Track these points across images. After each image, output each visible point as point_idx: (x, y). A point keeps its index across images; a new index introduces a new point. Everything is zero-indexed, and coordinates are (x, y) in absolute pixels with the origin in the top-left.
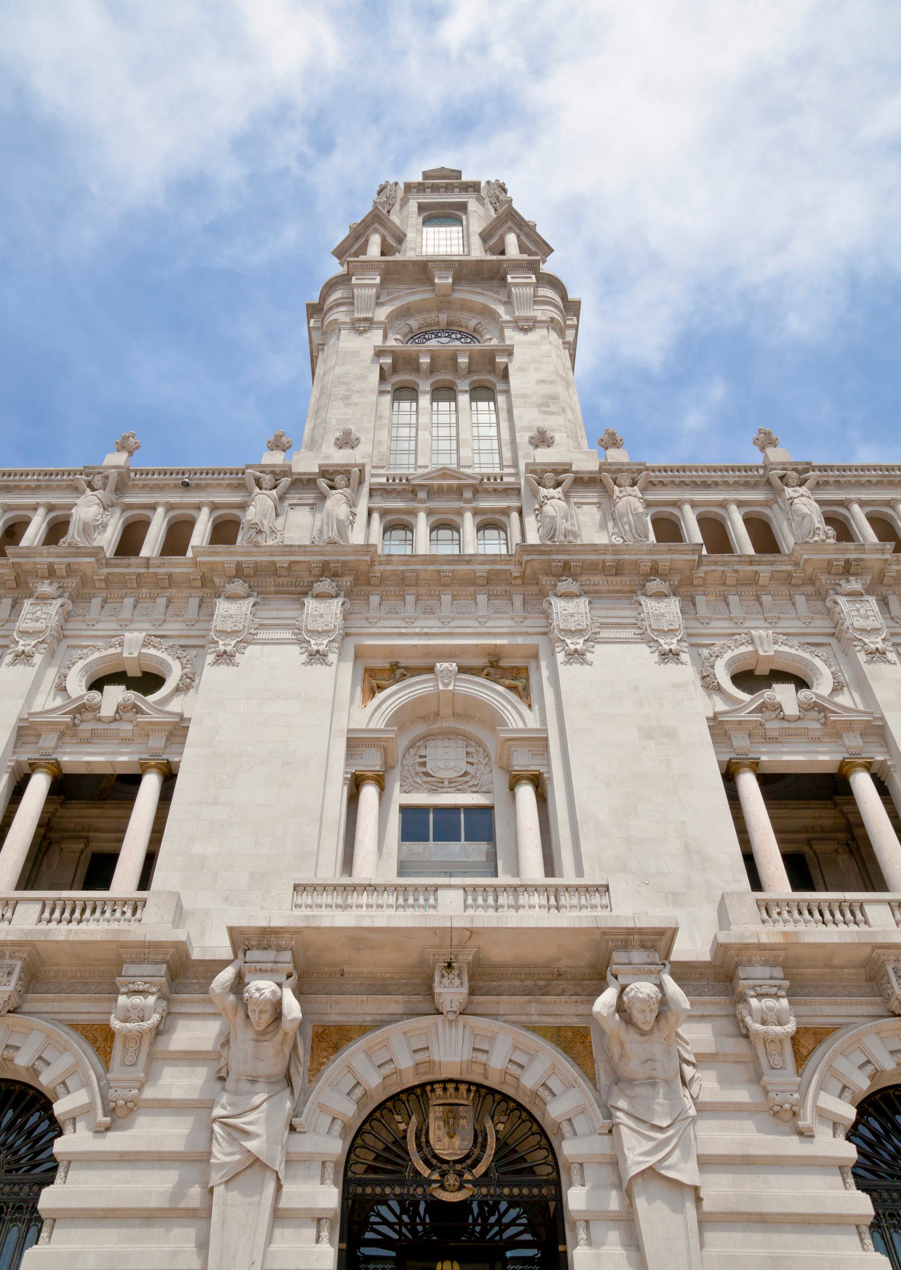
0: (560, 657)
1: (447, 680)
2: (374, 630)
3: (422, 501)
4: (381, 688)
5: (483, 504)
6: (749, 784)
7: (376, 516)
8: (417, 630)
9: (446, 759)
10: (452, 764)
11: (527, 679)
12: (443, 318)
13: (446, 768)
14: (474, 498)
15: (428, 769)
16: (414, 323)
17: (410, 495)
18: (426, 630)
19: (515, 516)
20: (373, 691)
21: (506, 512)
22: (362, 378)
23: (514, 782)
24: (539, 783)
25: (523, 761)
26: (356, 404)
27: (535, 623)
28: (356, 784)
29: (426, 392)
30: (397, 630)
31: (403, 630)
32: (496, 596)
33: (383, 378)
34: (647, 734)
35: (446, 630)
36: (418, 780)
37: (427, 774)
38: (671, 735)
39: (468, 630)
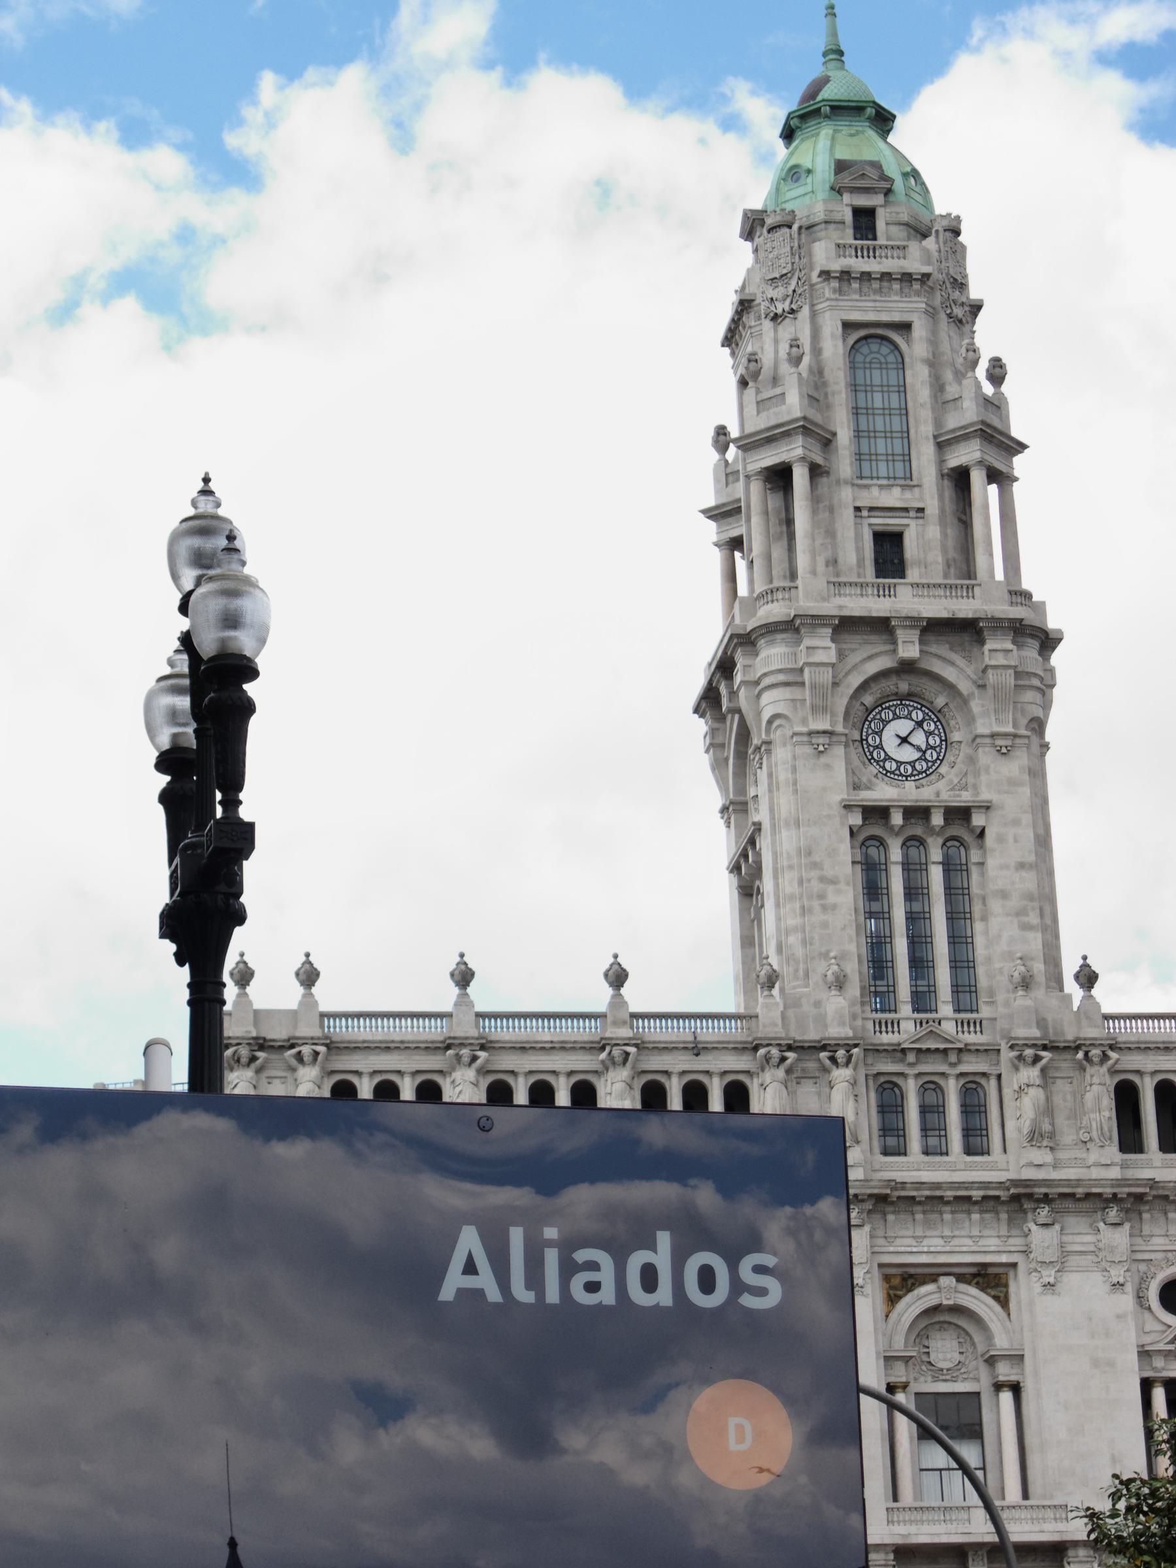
0: (1038, 1288)
1: (945, 1291)
2: (892, 1249)
3: (911, 1065)
4: (900, 1298)
5: (964, 1068)
6: (1159, 1396)
7: (871, 1082)
8: (925, 1249)
9: (944, 1349)
10: (949, 1356)
11: (1006, 1286)
12: (904, 687)
13: (945, 1360)
14: (959, 1062)
15: (931, 1360)
16: (868, 700)
17: (899, 1055)
18: (932, 1249)
19: (993, 1082)
20: (892, 1299)
21: (984, 1074)
22: (832, 853)
23: (998, 1387)
24: (1016, 1389)
25: (1005, 1372)
26: (834, 907)
27: (1016, 1242)
29: (897, 863)
30: (909, 1249)
31: (915, 1250)
32: (987, 1211)
33: (852, 834)
34: (1096, 1363)
35: (948, 1249)
36: (924, 1368)
37: (930, 1363)
38: (1111, 1364)
39: (964, 1249)
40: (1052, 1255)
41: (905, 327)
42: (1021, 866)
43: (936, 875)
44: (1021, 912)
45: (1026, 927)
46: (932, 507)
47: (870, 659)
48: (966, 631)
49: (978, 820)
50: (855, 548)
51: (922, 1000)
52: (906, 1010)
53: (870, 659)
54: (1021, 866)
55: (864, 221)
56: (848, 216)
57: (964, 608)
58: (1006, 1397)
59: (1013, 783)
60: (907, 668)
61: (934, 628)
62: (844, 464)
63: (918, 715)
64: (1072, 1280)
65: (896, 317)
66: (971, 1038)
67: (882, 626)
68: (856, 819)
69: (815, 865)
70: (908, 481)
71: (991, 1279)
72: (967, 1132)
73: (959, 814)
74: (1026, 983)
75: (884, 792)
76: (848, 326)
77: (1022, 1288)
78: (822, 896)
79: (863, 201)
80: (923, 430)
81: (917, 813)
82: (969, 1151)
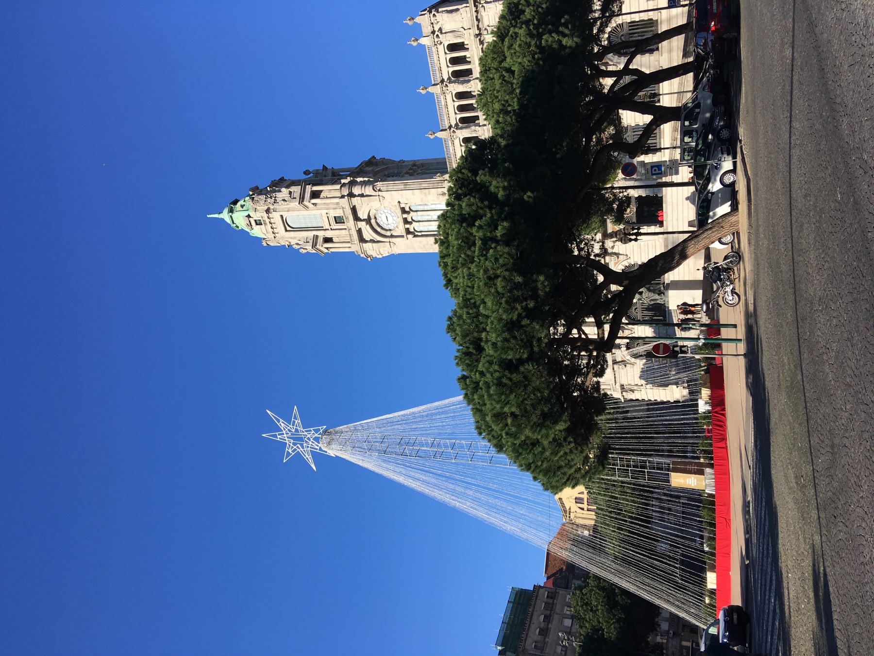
22: (420, 242)
41: (282, 216)
45: (429, 193)
47: (368, 233)
48: (354, 210)
49: (402, 206)
57: (349, 213)
60: (368, 221)
61: (357, 218)
62: (321, 234)
67: (359, 232)
68: (410, 236)
73: (403, 211)
76: (286, 231)
79: (253, 223)
81: (406, 221)
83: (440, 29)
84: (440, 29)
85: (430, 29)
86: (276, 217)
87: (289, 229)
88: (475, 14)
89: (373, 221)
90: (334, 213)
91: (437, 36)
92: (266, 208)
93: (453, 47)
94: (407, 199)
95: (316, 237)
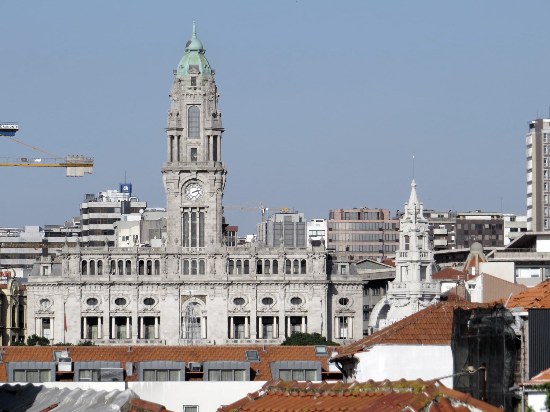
1: (193, 299)
20: (184, 301)
22: (177, 217)
24: (206, 318)
25: (205, 314)
28: (182, 318)
40: (213, 294)
42: (214, 219)
43: (198, 219)
44: (213, 228)
45: (214, 231)
46: (202, 144)
50: (186, 153)
51: (194, 244)
52: (190, 246)
53: (185, 177)
54: (214, 219)
55: (194, 80)
56: (190, 79)
58: (204, 319)
59: (213, 202)
63: (197, 187)
64: (216, 299)
65: (198, 103)
66: (203, 252)
68: (182, 210)
69: (174, 219)
70: (198, 137)
71: (202, 297)
72: (200, 270)
74: (212, 242)
75: (188, 204)
77: (208, 299)
78: (175, 225)
79: (194, 75)
80: (202, 127)
82: (200, 273)
83: (315, 258)
84: (315, 258)
85: (316, 252)
86: (200, 100)
87: (189, 106)
88: (321, 282)
89: (194, 182)
90: (200, 149)
91: (312, 256)
92: (207, 93)
93: (304, 263)
94: (210, 213)
95: (181, 130)
